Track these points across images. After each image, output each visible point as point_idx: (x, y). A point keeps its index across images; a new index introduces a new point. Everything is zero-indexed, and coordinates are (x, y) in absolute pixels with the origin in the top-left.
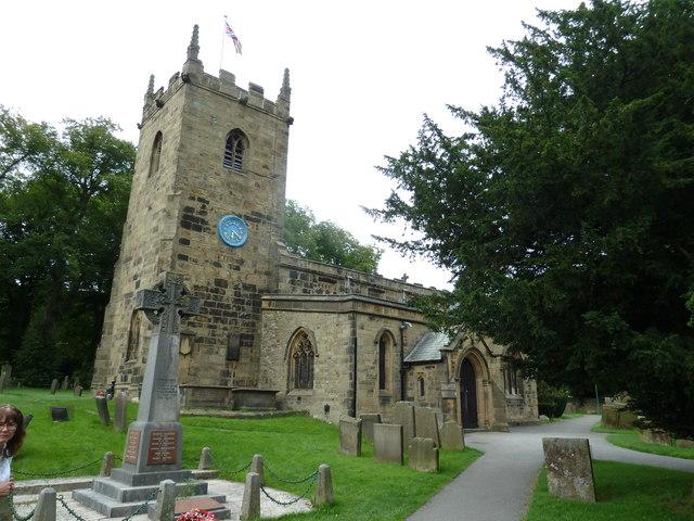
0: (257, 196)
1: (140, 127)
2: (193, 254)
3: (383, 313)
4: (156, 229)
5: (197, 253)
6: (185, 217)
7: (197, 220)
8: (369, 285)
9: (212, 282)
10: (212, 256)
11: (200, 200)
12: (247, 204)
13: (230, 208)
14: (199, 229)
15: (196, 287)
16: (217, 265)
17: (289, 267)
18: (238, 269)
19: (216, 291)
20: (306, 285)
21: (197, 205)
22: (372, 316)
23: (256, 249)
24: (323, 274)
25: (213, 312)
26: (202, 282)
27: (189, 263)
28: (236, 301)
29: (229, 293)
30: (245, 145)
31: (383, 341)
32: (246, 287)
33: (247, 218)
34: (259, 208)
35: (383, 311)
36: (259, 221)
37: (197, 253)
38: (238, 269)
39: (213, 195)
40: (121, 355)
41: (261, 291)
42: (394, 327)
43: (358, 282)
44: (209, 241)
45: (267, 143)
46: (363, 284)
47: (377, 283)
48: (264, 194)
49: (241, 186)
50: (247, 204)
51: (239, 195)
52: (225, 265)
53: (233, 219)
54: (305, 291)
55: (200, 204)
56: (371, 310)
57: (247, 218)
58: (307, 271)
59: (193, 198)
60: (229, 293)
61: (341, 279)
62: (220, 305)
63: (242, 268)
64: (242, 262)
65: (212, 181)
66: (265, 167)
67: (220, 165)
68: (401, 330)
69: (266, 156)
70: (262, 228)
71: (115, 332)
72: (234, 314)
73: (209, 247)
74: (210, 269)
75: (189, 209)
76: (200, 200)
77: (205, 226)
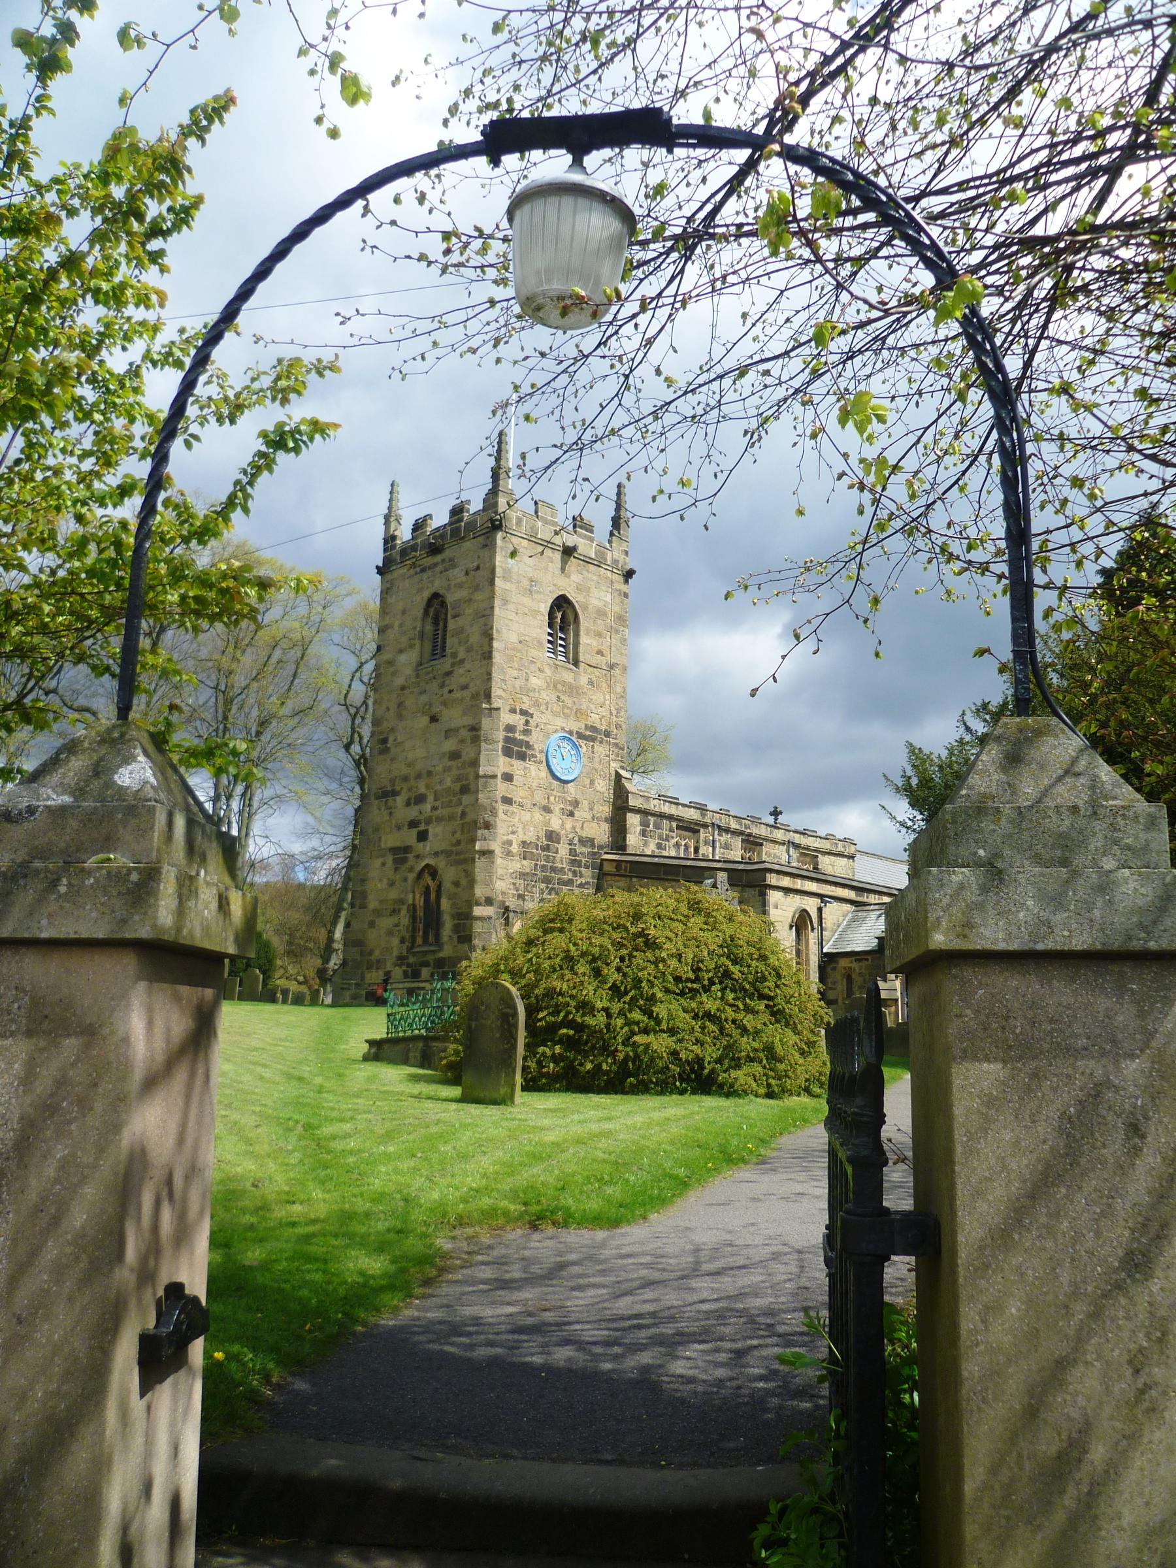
0: (590, 700)
1: (380, 571)
2: (519, 795)
3: (799, 887)
4: (455, 755)
5: (522, 793)
6: (507, 740)
7: (520, 743)
8: (740, 833)
9: (542, 834)
10: (539, 797)
11: (524, 712)
12: (579, 713)
13: (559, 722)
14: (522, 757)
15: (524, 842)
16: (547, 809)
17: (638, 811)
18: (571, 814)
19: (547, 848)
20: (660, 838)
21: (518, 720)
22: (787, 891)
23: (592, 782)
24: (679, 819)
25: (547, 880)
26: (530, 837)
27: (513, 808)
28: (573, 862)
29: (563, 850)
30: (571, 618)
31: (801, 922)
32: (582, 841)
33: (580, 736)
34: (594, 720)
35: (799, 884)
36: (593, 739)
37: (522, 793)
38: (571, 814)
39: (537, 704)
40: (395, 942)
41: (601, 847)
42: (811, 905)
43: (727, 830)
44: (535, 773)
45: (601, 613)
46: (736, 833)
47: (754, 830)
48: (597, 697)
49: (570, 686)
50: (579, 713)
51: (568, 700)
52: (556, 809)
53: (564, 738)
54: (659, 846)
55: (524, 718)
56: (786, 882)
57: (580, 736)
58: (662, 816)
59: (513, 711)
60: (563, 850)
61: (705, 826)
62: (553, 869)
63: (577, 813)
64: (576, 803)
65: (535, 681)
66: (600, 652)
67: (543, 655)
68: (820, 910)
69: (599, 635)
70: (600, 749)
71: (373, 904)
72: (570, 882)
73: (535, 784)
74: (538, 816)
75: (510, 728)
76: (524, 712)
77: (529, 752)
